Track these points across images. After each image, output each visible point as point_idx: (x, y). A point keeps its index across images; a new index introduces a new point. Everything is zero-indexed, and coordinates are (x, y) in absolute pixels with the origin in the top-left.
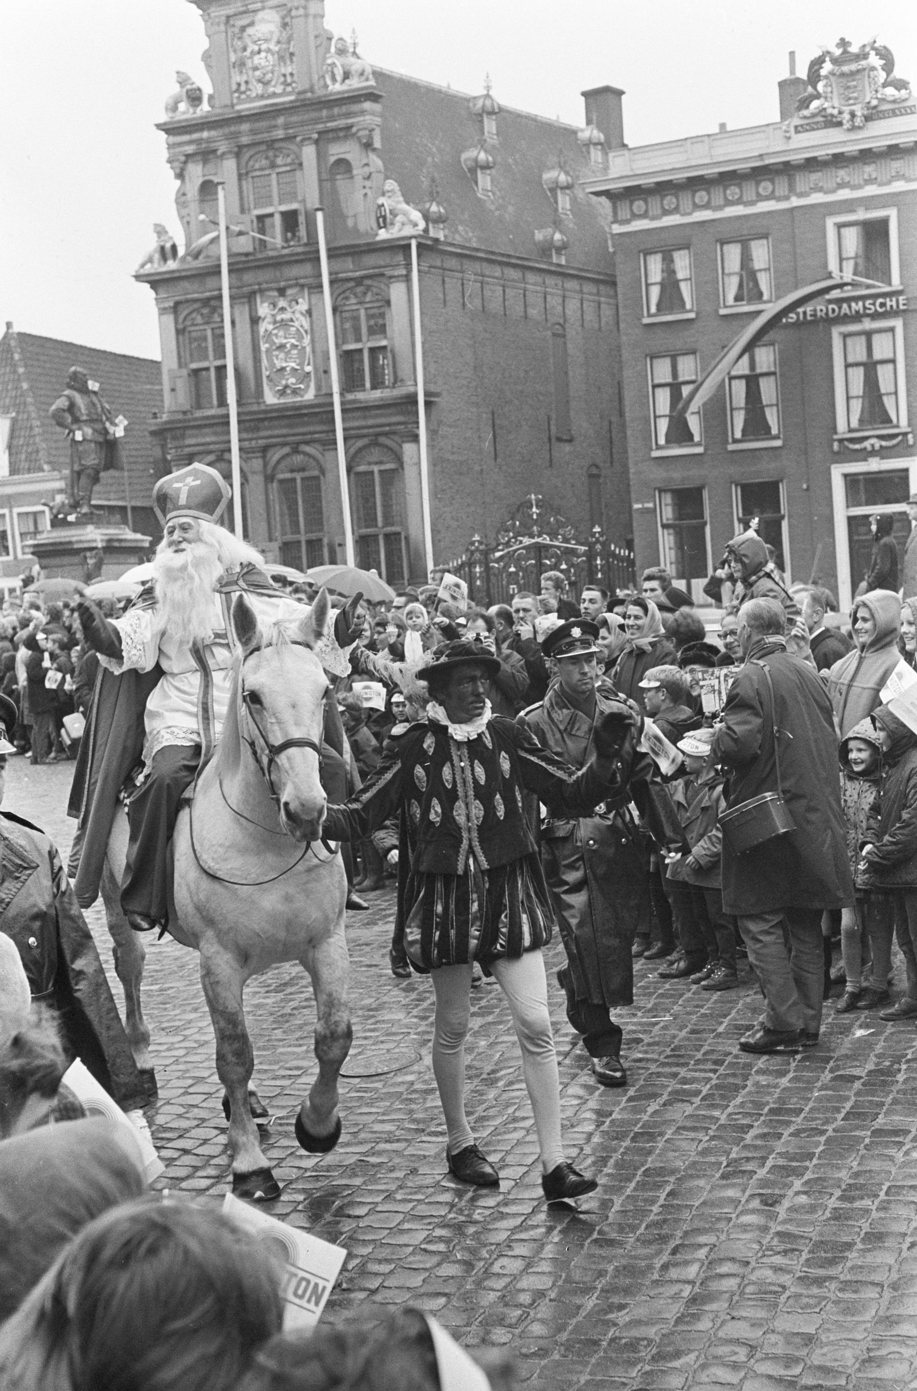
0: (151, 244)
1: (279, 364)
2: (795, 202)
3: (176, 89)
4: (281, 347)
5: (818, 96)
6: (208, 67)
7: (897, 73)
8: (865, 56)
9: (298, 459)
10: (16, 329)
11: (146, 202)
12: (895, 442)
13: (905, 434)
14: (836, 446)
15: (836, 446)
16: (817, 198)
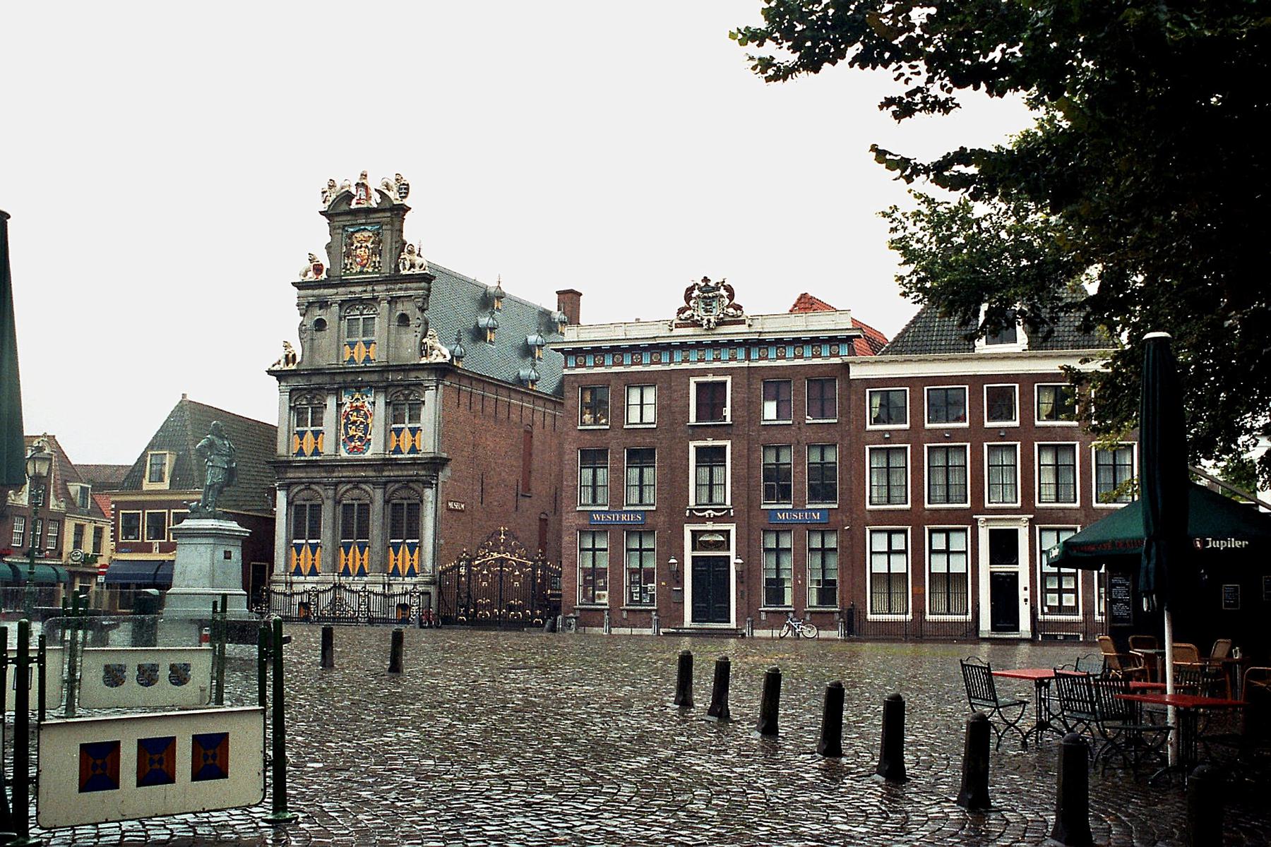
0: (281, 355)
1: (351, 433)
2: (673, 366)
5: (690, 308)
6: (329, 253)
7: (736, 301)
8: (718, 289)
10: (189, 398)
11: (279, 329)
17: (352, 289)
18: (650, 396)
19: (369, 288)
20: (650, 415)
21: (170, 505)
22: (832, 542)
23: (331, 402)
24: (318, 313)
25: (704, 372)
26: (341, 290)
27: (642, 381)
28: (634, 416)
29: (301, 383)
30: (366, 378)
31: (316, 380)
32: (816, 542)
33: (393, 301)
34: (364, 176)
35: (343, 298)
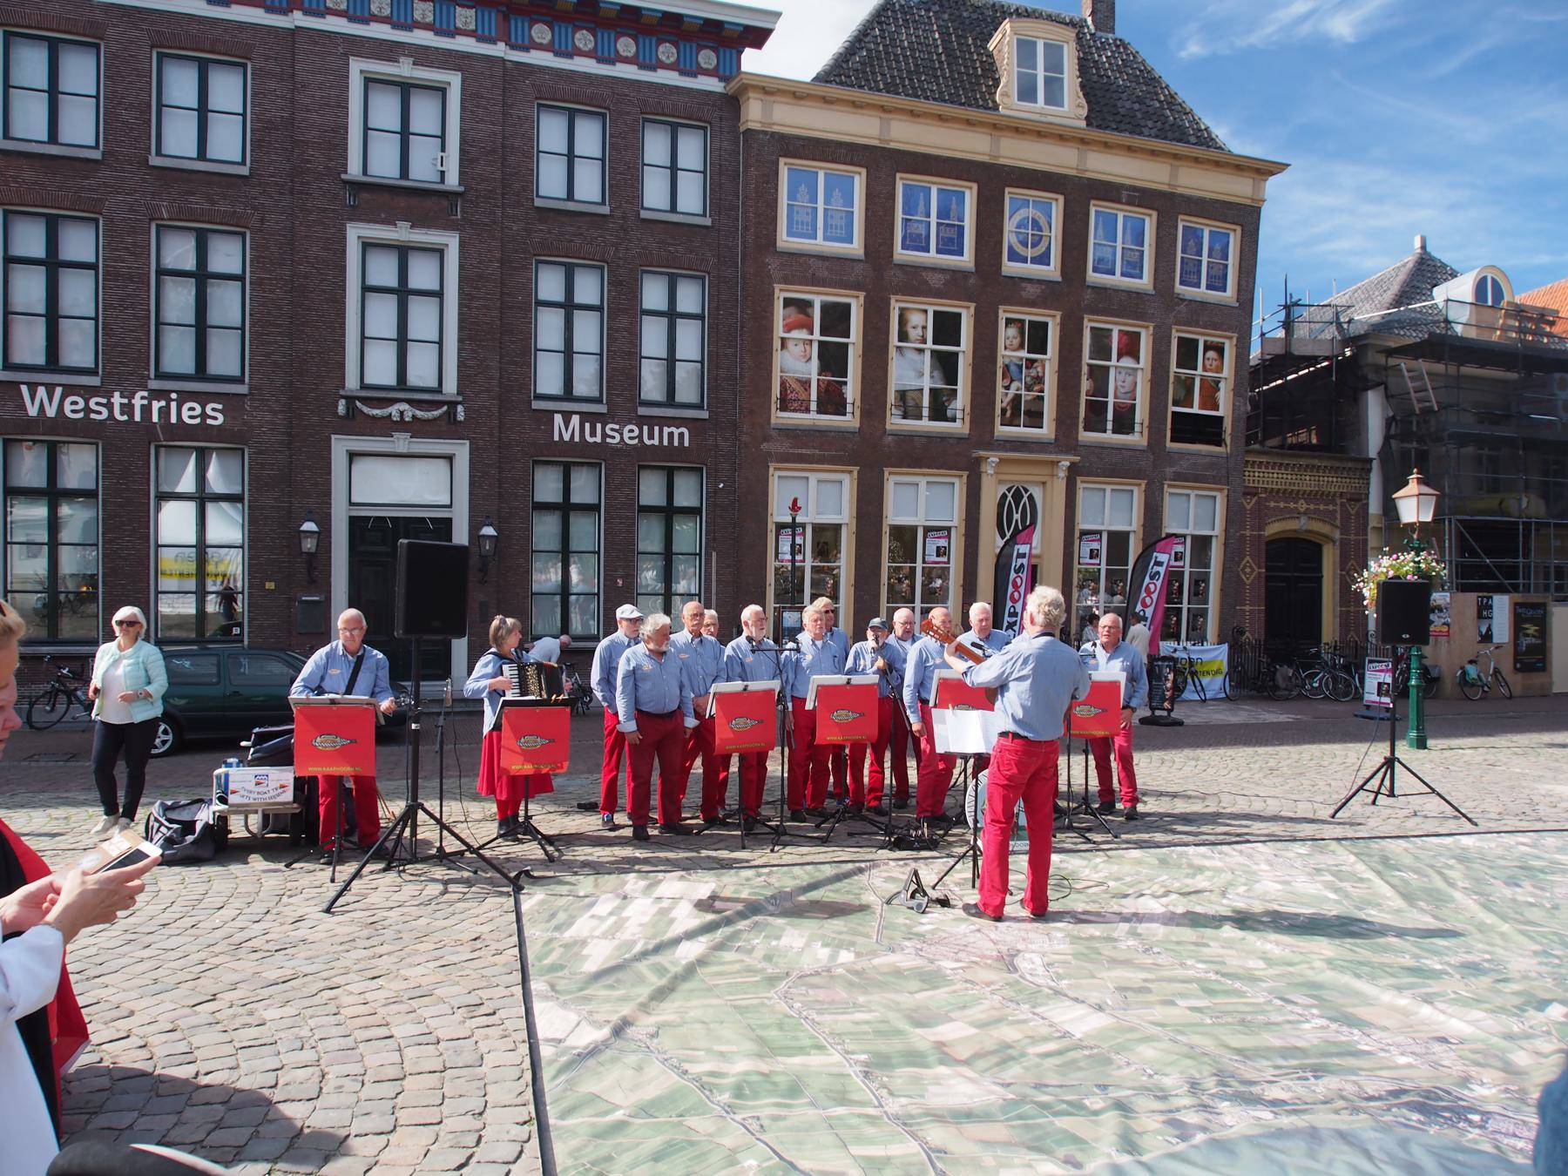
12: (436, 413)
13: (452, 405)
14: (341, 408)
15: (341, 408)
18: (228, 90)
20: (228, 143)
22: (687, 493)
25: (389, 51)
28: (179, 139)
32: (651, 491)
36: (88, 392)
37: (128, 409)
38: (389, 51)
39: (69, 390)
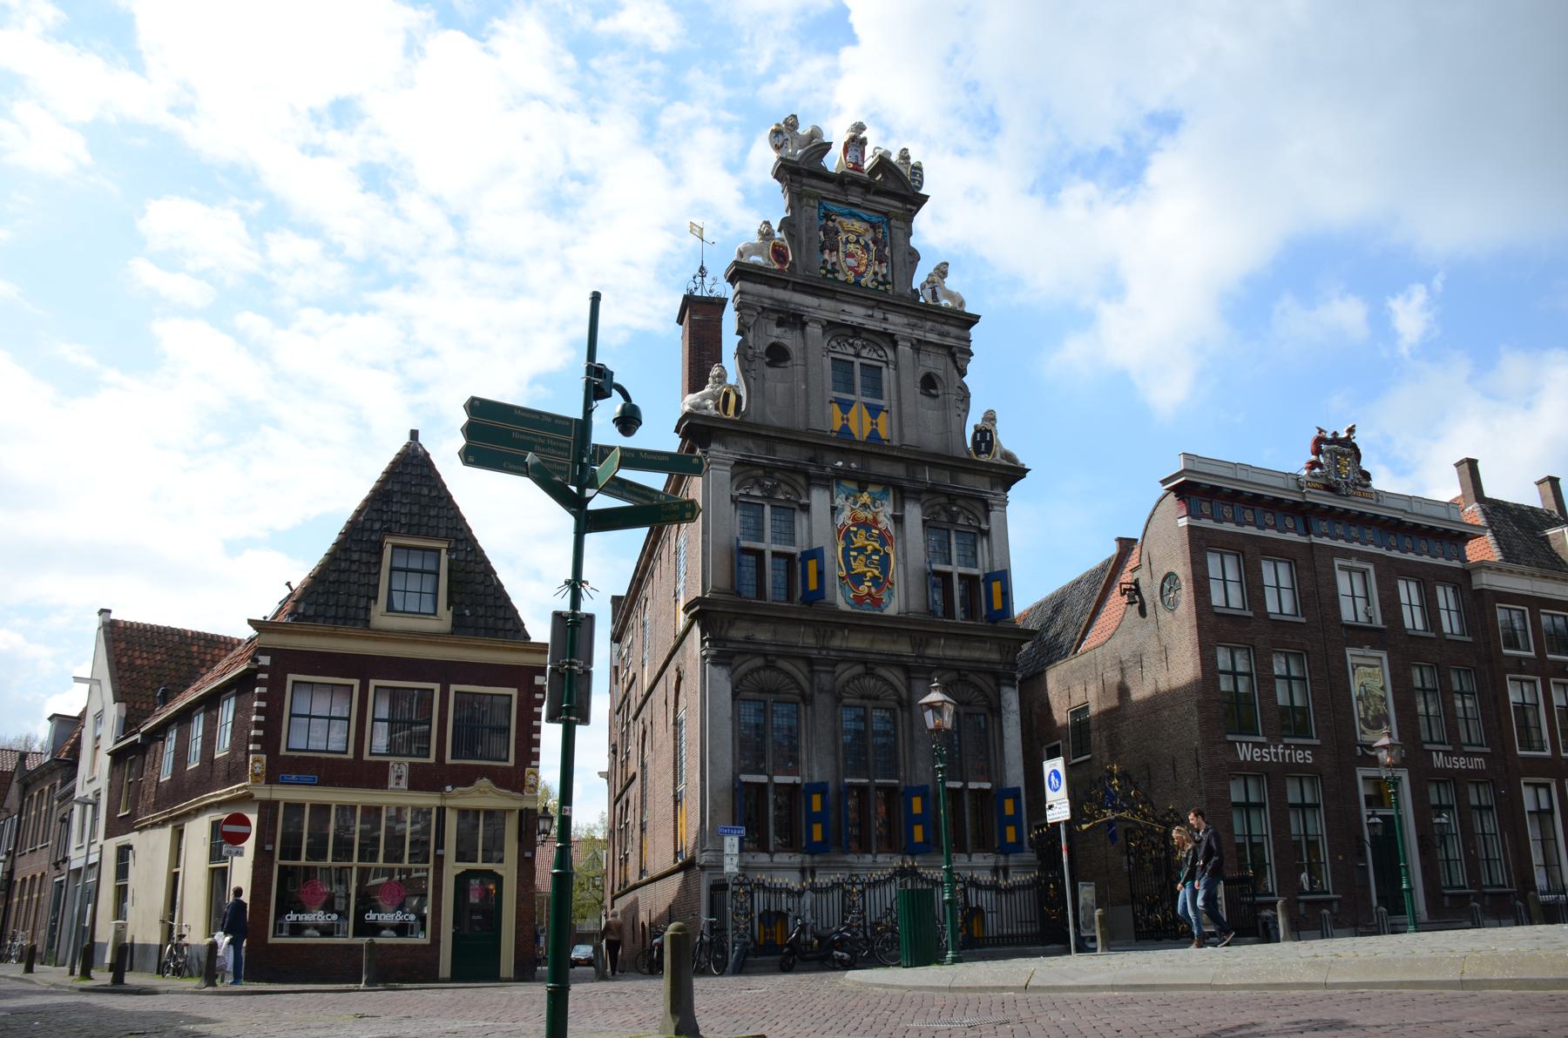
1: (859, 567)
2: (1315, 540)
3: (756, 239)
4: (864, 548)
9: (869, 683)
16: (1325, 541)
17: (846, 307)
19: (878, 314)
21: (447, 672)
23: (819, 499)
24: (776, 333)
25: (1347, 554)
26: (825, 303)
27: (1275, 551)
29: (758, 453)
30: (883, 469)
31: (785, 454)
33: (919, 346)
34: (860, 127)
35: (832, 317)
36: (1261, 746)
37: (1276, 754)
38: (1347, 554)
39: (1256, 745)
